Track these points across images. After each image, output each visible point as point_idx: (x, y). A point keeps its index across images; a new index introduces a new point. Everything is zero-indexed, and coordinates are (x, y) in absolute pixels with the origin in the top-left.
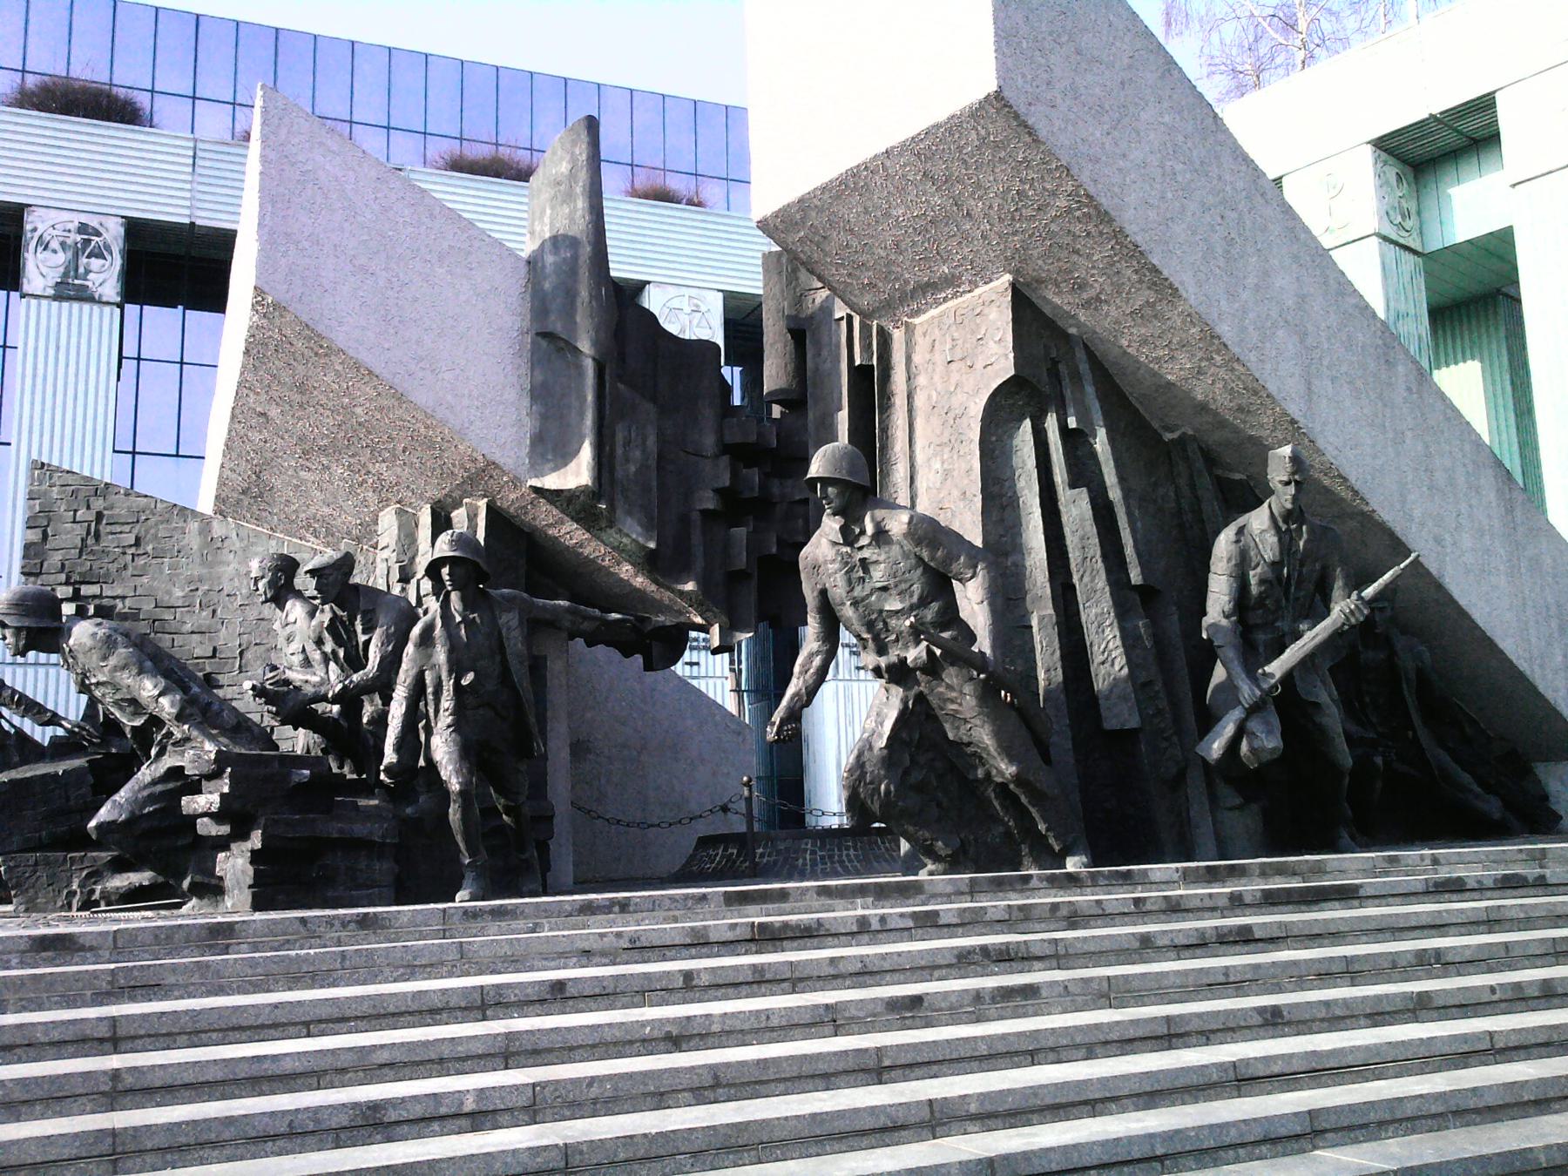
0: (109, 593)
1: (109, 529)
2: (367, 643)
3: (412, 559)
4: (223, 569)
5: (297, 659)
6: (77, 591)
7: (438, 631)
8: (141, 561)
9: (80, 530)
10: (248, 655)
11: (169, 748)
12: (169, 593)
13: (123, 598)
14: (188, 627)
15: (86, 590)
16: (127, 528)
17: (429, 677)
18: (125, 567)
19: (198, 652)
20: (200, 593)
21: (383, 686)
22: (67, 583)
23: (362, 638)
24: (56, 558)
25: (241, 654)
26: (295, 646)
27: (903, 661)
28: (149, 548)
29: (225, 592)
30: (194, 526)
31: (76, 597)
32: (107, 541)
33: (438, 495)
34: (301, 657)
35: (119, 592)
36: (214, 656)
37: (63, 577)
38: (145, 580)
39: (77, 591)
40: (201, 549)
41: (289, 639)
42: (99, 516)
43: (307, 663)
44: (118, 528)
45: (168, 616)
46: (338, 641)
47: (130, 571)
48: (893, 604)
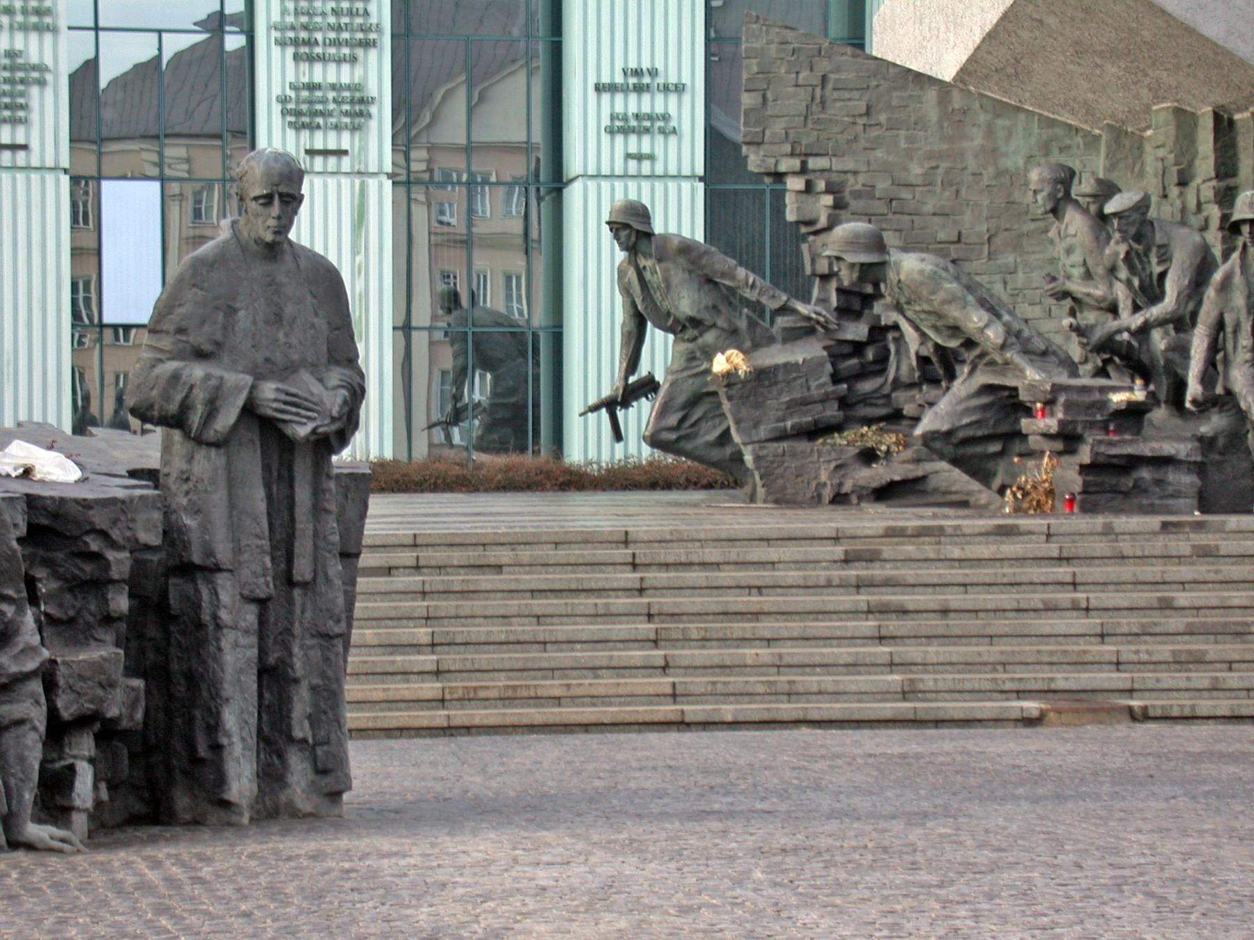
0: (840, 168)
1: (836, 95)
2: (1162, 276)
3: (1191, 164)
4: (965, 144)
5: (1077, 272)
6: (804, 164)
7: (1238, 279)
8: (874, 133)
9: (804, 94)
10: (997, 241)
11: (980, 367)
12: (906, 169)
13: (855, 173)
14: (929, 208)
15: (813, 163)
16: (856, 95)
17: (1229, 320)
18: (856, 139)
19: (942, 236)
20: (941, 171)
21: (1182, 323)
22: (792, 154)
23: (1157, 269)
24: (778, 127)
25: (989, 239)
26: (1077, 257)
28: (883, 118)
29: (970, 171)
30: (932, 95)
31: (804, 170)
32: (835, 109)
33: (1221, 100)
34: (1082, 270)
35: (850, 165)
36: (959, 241)
37: (787, 148)
38: (879, 154)
39: (804, 164)
41: (1069, 251)
42: (824, 79)
43: (1088, 275)
44: (847, 95)
45: (905, 194)
46: (1132, 269)
47: (863, 143)
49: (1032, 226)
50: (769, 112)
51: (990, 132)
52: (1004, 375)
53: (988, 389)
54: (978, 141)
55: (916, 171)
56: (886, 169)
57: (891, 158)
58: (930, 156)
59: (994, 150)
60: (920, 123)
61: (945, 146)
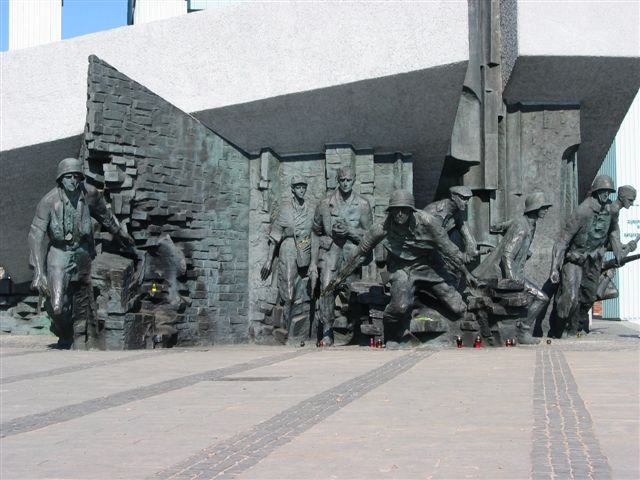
5: (354, 224)
8: (153, 136)
13: (143, 157)
14: (178, 182)
20: (184, 161)
27: (589, 256)
28: (158, 128)
30: (181, 119)
38: (156, 148)
40: (184, 134)
41: (351, 213)
44: (142, 112)
48: (598, 236)
49: (221, 196)
50: (104, 115)
51: (204, 144)
52: (426, 275)
53: (417, 283)
54: (200, 148)
55: (173, 160)
56: (159, 157)
57: (161, 151)
58: (181, 153)
59: (206, 153)
60: (175, 134)
61: (186, 149)
